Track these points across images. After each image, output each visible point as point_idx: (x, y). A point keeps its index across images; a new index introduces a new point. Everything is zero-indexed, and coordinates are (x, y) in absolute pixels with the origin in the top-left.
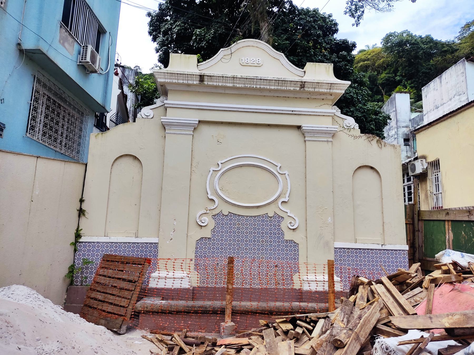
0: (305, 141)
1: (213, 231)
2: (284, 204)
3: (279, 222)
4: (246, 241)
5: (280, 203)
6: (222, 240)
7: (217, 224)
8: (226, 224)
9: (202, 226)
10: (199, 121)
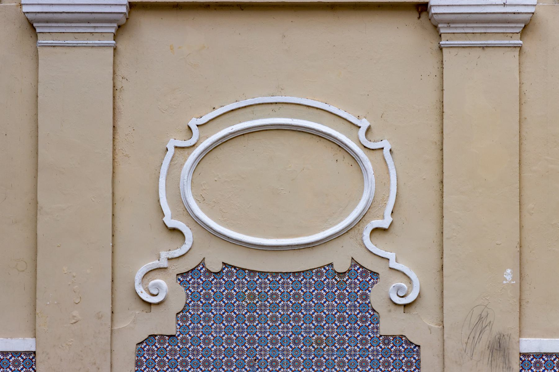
0: (441, 49)
1: (182, 315)
2: (376, 234)
3: (365, 286)
4: (274, 341)
5: (366, 234)
6: (206, 341)
7: (192, 297)
8: (218, 297)
9: (150, 304)
10: (132, 6)
